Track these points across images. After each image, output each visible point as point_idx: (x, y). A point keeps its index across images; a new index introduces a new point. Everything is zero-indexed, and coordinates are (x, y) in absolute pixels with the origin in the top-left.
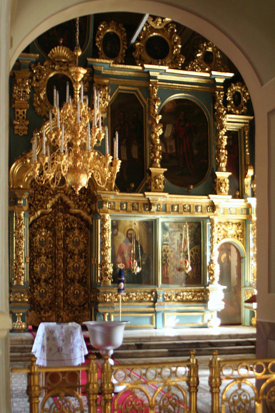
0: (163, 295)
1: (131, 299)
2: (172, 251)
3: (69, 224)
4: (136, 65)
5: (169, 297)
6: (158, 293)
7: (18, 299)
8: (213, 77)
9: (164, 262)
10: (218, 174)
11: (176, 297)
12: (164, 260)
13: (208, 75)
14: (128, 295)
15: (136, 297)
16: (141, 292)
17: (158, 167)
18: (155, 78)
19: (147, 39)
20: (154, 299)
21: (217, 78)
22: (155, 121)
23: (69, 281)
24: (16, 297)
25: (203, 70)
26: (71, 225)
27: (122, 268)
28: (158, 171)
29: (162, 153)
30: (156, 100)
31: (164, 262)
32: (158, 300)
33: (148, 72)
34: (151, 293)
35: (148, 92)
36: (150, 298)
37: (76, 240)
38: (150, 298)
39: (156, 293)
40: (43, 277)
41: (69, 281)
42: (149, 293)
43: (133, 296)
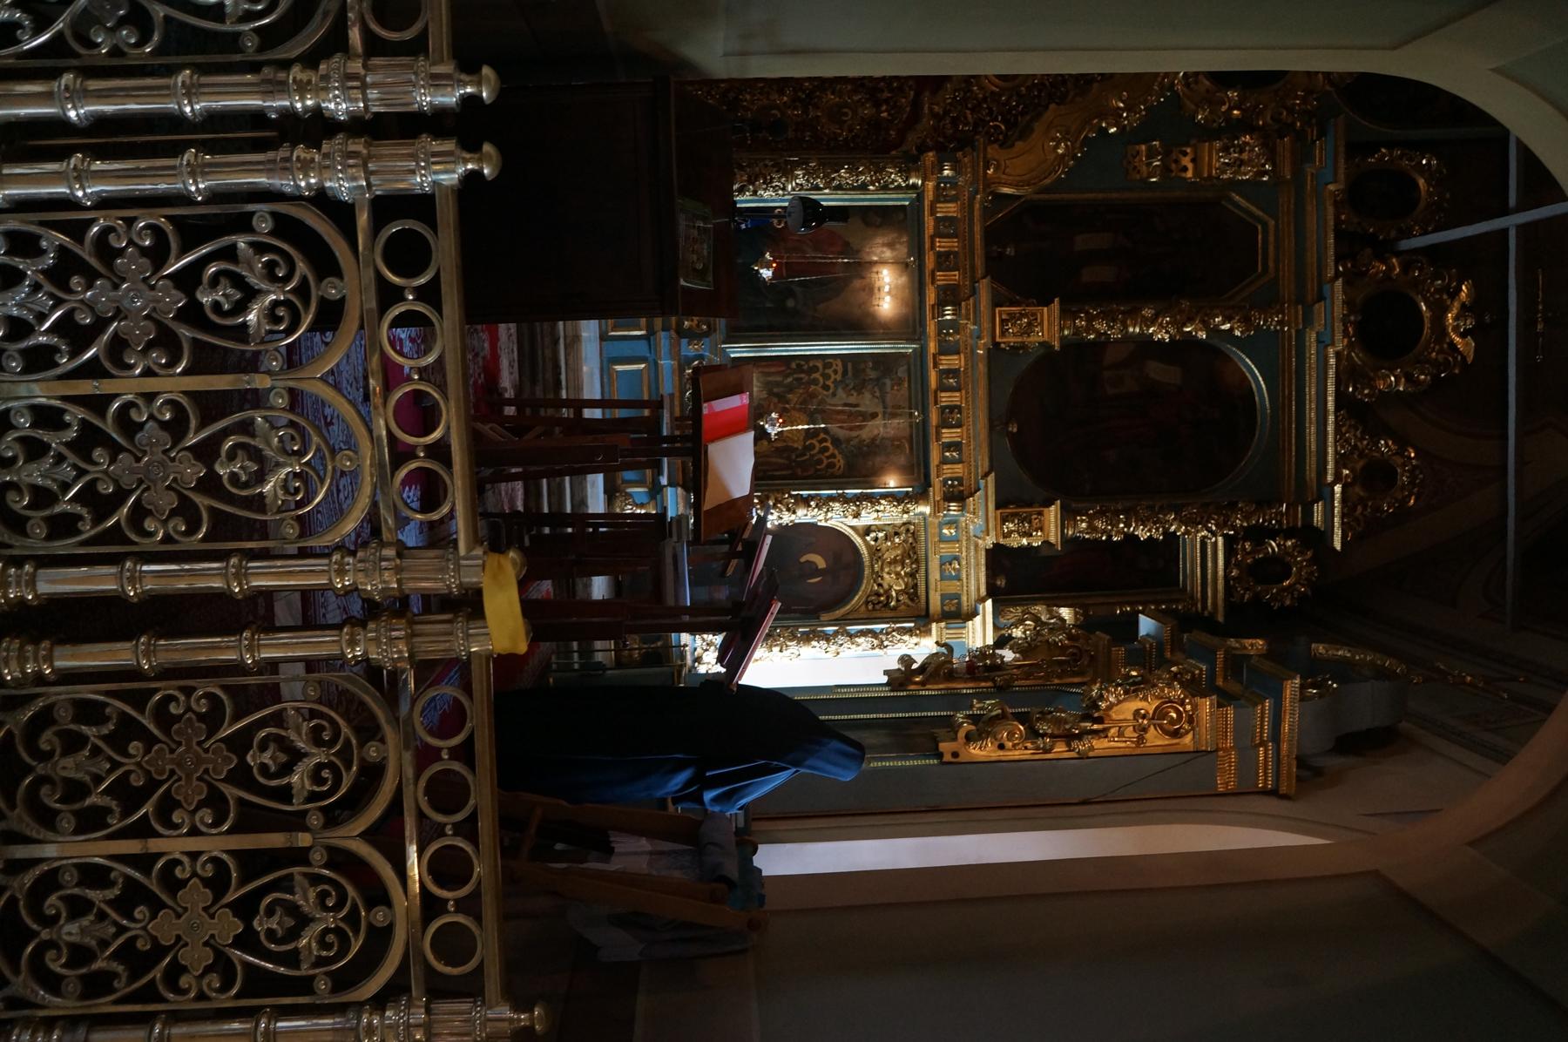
2: (826, 387)
3: (886, 94)
4: (1339, 259)
8: (1326, 490)
9: (794, 365)
10: (1052, 513)
12: (799, 366)
13: (1330, 478)
17: (1062, 329)
18: (1308, 321)
19: (1412, 294)
21: (1325, 507)
22: (1190, 320)
23: (731, 95)
25: (1341, 461)
26: (886, 101)
28: (1048, 327)
29: (1102, 344)
30: (1246, 321)
31: (794, 365)
32: (684, 341)
33: (1321, 298)
35: (1270, 302)
37: (846, 114)
39: (706, 334)
41: (731, 95)
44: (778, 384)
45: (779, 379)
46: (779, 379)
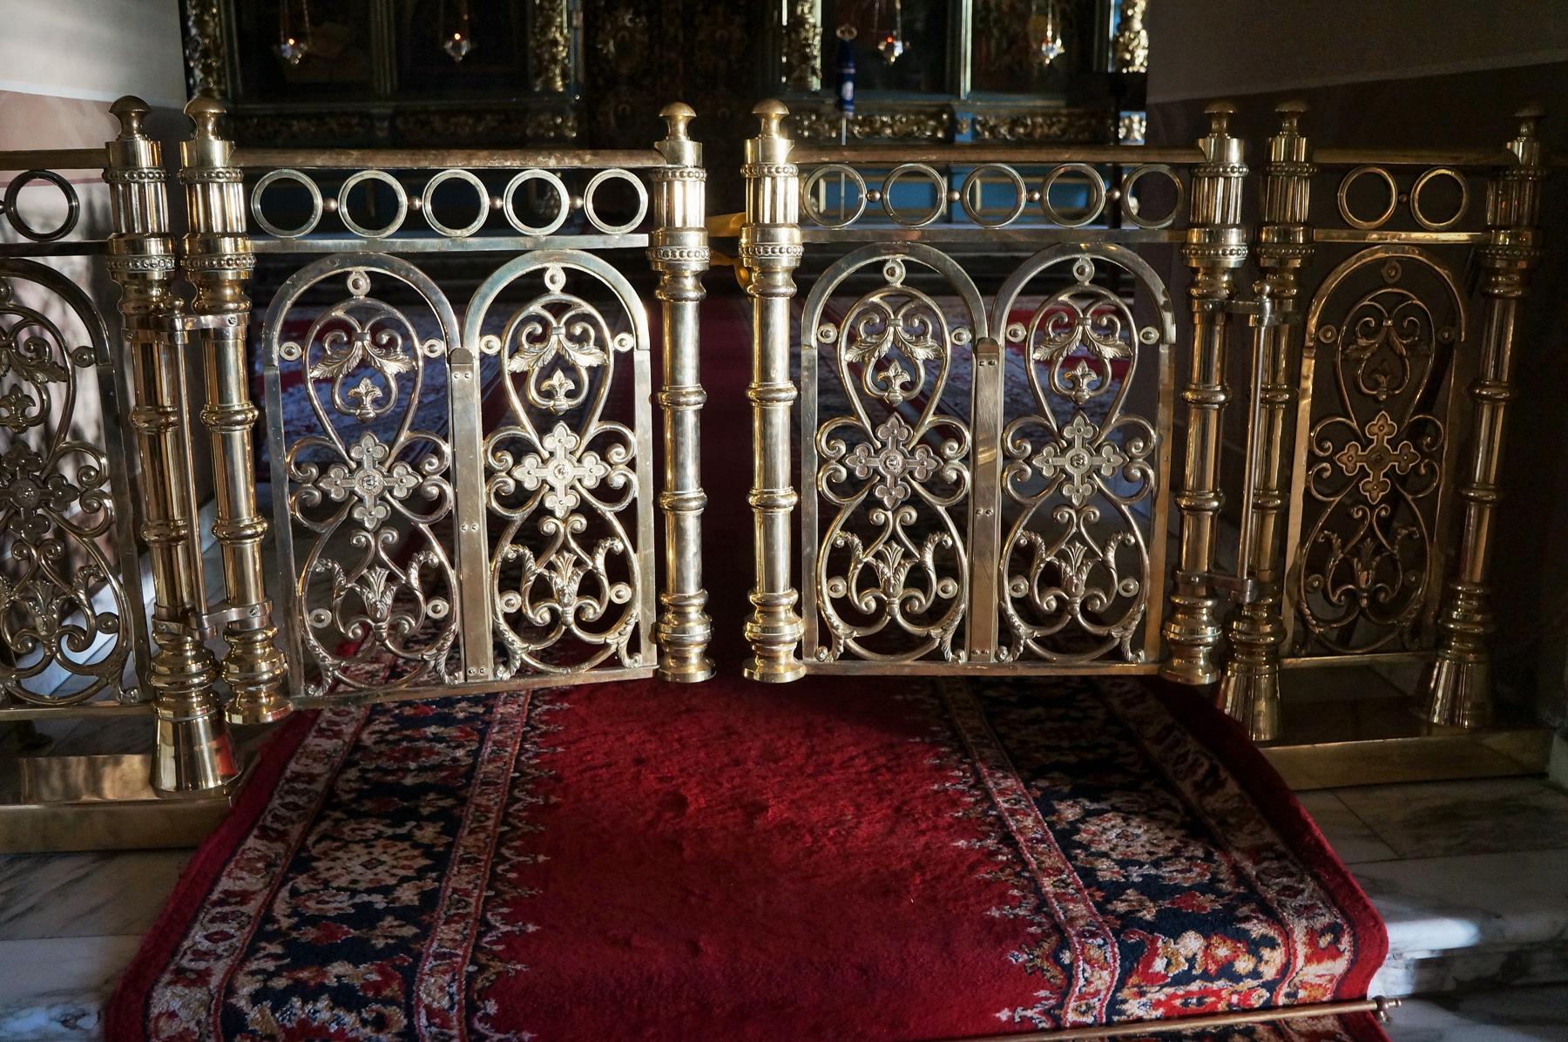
0: (974, 122)
1: (878, 132)
5: (992, 130)
6: (958, 116)
7: (548, 129)
9: (980, 26)
11: (1011, 131)
12: (982, 20)
14: (868, 121)
15: (891, 126)
16: (906, 113)
20: (946, 132)
24: (540, 125)
27: (847, 38)
34: (936, 116)
36: (934, 131)
38: (934, 131)
40: (624, 70)
42: (931, 116)
43: (884, 124)
44: (999, 44)
45: (993, 43)
46: (993, 43)
